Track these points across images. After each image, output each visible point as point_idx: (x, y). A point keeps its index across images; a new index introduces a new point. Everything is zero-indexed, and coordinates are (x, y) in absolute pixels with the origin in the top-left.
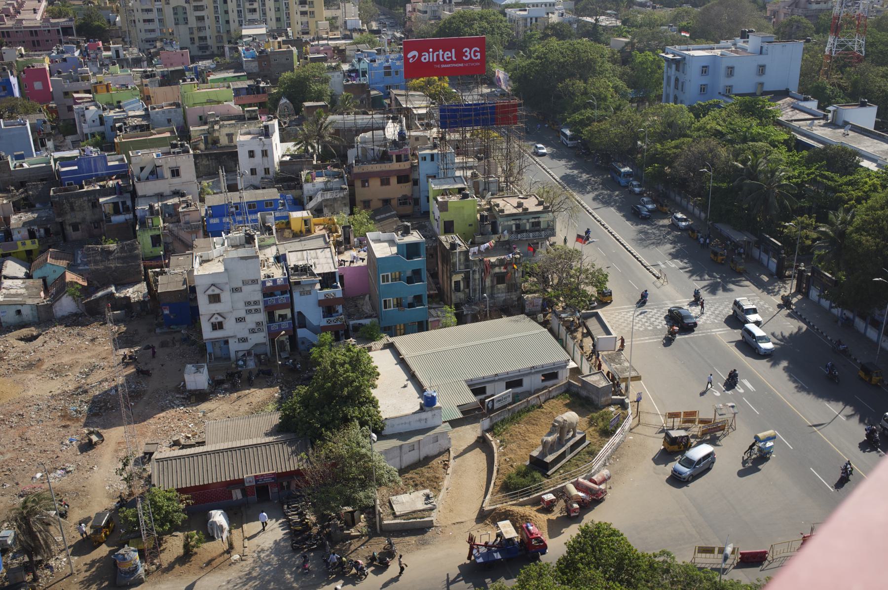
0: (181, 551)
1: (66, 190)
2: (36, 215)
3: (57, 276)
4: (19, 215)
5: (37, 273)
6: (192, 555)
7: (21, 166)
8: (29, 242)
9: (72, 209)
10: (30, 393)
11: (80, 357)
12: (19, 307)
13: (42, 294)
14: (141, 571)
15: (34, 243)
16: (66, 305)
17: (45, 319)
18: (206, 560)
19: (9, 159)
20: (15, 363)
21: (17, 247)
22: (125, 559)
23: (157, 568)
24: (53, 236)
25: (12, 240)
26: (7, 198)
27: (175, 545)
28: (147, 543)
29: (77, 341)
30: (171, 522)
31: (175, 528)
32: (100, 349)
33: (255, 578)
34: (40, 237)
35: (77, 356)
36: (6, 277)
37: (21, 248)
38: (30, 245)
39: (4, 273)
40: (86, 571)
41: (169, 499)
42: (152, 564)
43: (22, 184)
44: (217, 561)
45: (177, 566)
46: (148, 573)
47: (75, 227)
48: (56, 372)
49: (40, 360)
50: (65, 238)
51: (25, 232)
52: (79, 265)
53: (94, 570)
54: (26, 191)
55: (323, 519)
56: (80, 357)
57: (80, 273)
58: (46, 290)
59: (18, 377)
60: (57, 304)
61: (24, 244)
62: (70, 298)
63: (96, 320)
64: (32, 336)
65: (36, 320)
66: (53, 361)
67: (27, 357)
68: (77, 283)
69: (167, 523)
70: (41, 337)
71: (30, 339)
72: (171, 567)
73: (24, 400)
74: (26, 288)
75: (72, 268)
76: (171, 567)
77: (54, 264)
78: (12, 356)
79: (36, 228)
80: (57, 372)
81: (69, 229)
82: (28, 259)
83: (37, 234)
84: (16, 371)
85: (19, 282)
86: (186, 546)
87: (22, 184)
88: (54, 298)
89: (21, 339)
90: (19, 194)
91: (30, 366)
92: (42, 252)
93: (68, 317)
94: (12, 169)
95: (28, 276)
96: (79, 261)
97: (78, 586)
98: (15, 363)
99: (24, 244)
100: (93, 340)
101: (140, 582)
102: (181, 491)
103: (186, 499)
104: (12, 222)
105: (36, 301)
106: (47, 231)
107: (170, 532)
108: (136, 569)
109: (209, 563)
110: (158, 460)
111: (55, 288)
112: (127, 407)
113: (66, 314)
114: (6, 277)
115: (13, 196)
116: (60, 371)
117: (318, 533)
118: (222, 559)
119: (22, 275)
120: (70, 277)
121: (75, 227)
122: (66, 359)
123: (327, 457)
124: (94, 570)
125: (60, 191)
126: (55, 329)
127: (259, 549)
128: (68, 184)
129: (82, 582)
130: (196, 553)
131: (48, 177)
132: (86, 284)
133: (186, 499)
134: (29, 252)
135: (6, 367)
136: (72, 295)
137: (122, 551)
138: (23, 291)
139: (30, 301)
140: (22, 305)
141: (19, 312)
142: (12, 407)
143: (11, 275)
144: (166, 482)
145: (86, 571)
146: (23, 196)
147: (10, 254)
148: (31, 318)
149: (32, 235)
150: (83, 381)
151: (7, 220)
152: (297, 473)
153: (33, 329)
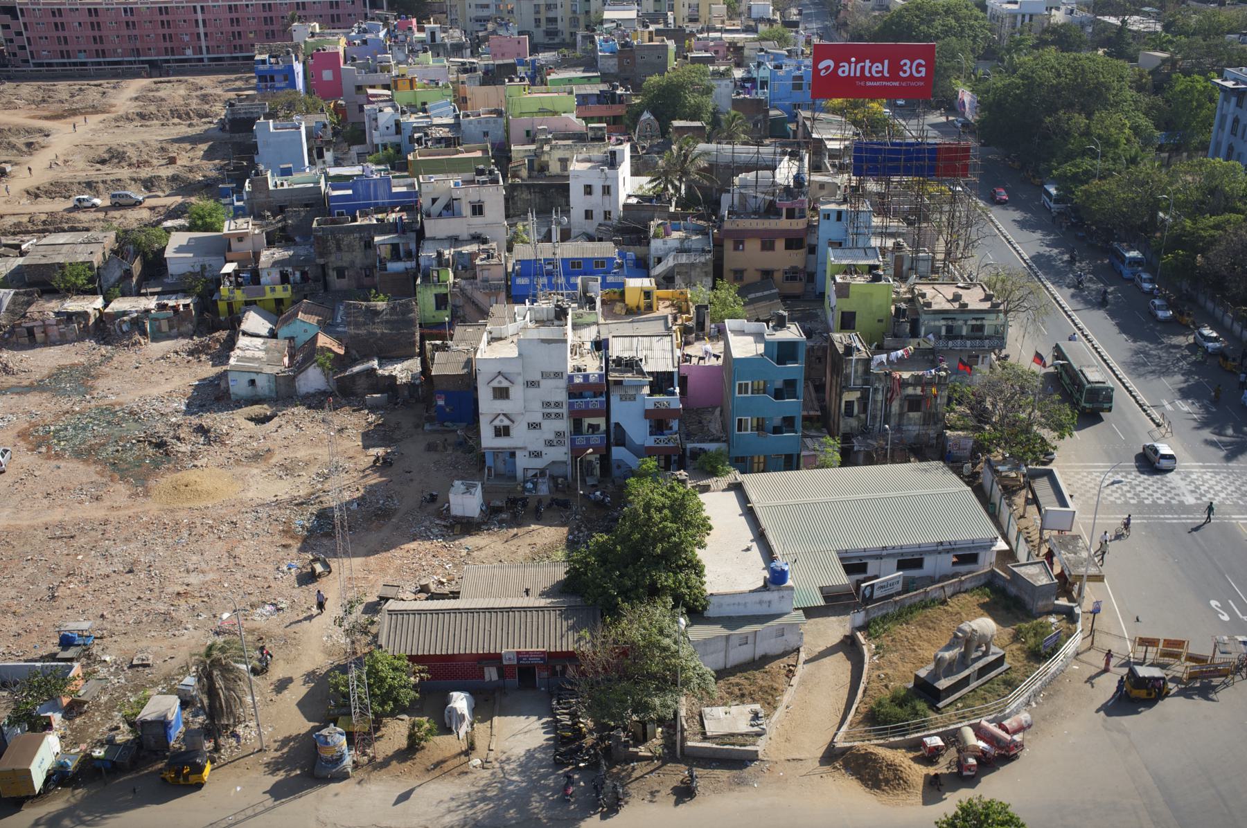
0: (403, 743)
1: (333, 222)
2: (291, 253)
3: (308, 337)
4: (273, 250)
5: (284, 331)
6: (418, 750)
7: (282, 184)
8: (279, 288)
9: (339, 248)
10: (250, 495)
11: (320, 452)
12: (253, 376)
13: (286, 360)
14: (348, 761)
15: (285, 290)
16: (313, 379)
17: (283, 394)
18: (435, 761)
19: (269, 174)
20: (237, 450)
21: (264, 294)
22: (327, 743)
23: (370, 761)
24: (312, 284)
25: (258, 283)
26: (260, 226)
27: (396, 733)
28: (358, 726)
29: (320, 430)
30: (396, 700)
31: (399, 709)
32: (347, 444)
33: (490, 799)
34: (295, 283)
35: (317, 451)
36: (244, 333)
37: (269, 296)
38: (281, 292)
39: (244, 327)
40: (276, 750)
41: (395, 669)
42: (364, 754)
43: (281, 209)
44: (450, 764)
45: (394, 763)
46: (356, 765)
47: (341, 273)
48: (287, 469)
49: (269, 450)
50: (326, 286)
51: (276, 275)
52: (338, 325)
53: (285, 750)
54: (284, 219)
55: (601, 727)
56: (320, 452)
57: (339, 338)
58: (291, 357)
59: (238, 470)
60: (301, 376)
61: (273, 290)
62: (319, 370)
63: (349, 404)
64: (266, 416)
65: (273, 395)
66: (286, 453)
67: (255, 444)
68: (330, 350)
69: (387, 702)
70: (276, 419)
71: (261, 420)
72: (386, 763)
73: (242, 503)
74: (266, 350)
75: (328, 327)
76: (386, 763)
77: (306, 321)
78: (236, 441)
79: (290, 270)
80: (288, 469)
81: (332, 275)
82: (277, 312)
83: (291, 278)
84: (238, 462)
85: (259, 341)
86: (412, 737)
87: (281, 209)
88: (298, 368)
89: (251, 419)
90: (275, 222)
91: (256, 457)
92: (294, 303)
93: (314, 395)
94: (271, 187)
95: (273, 335)
96: (339, 320)
97: (262, 768)
98: (237, 450)
99: (273, 290)
100: (341, 430)
101: (344, 776)
102: (413, 658)
103: (420, 672)
104: (263, 259)
105: (276, 370)
106: (304, 275)
107: (392, 714)
108: (341, 758)
109: (438, 764)
110: (391, 612)
111: (303, 354)
112: (344, 540)
113: (312, 391)
114: (244, 333)
115: (267, 225)
116: (293, 469)
117: (592, 746)
118: (456, 762)
119: (265, 332)
120: (324, 340)
121: (341, 273)
122: (302, 453)
123: (615, 642)
124: (285, 750)
125: (326, 223)
126: (295, 410)
127: (504, 758)
128: (339, 214)
129: (268, 765)
130: (423, 748)
131: (315, 202)
132: (342, 352)
133: (420, 672)
134: (279, 302)
135: (227, 454)
136: (322, 365)
137: (324, 732)
138: (261, 354)
139: (268, 370)
140: (257, 373)
141: (252, 382)
142: (224, 511)
143: (251, 330)
144: (396, 644)
145: (276, 750)
146: (280, 225)
147: (255, 303)
148: (267, 392)
149: (284, 279)
150: (319, 486)
151: (257, 255)
152: (570, 656)
153: (265, 406)
